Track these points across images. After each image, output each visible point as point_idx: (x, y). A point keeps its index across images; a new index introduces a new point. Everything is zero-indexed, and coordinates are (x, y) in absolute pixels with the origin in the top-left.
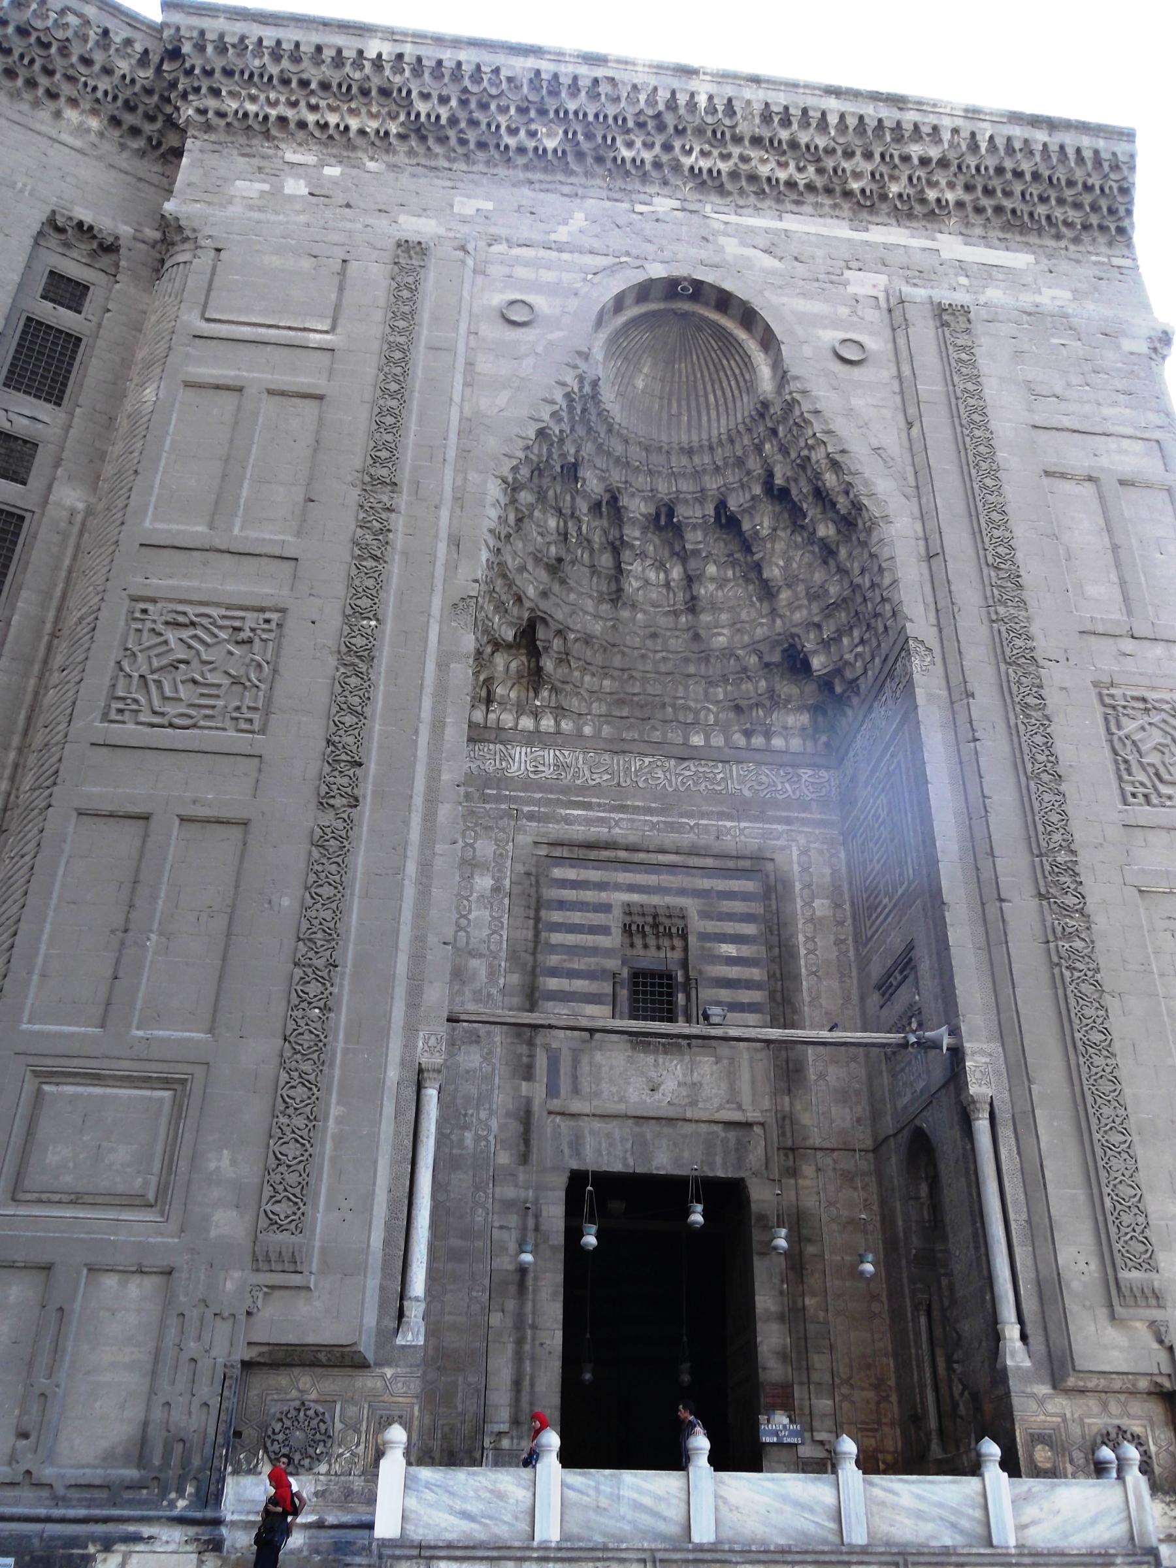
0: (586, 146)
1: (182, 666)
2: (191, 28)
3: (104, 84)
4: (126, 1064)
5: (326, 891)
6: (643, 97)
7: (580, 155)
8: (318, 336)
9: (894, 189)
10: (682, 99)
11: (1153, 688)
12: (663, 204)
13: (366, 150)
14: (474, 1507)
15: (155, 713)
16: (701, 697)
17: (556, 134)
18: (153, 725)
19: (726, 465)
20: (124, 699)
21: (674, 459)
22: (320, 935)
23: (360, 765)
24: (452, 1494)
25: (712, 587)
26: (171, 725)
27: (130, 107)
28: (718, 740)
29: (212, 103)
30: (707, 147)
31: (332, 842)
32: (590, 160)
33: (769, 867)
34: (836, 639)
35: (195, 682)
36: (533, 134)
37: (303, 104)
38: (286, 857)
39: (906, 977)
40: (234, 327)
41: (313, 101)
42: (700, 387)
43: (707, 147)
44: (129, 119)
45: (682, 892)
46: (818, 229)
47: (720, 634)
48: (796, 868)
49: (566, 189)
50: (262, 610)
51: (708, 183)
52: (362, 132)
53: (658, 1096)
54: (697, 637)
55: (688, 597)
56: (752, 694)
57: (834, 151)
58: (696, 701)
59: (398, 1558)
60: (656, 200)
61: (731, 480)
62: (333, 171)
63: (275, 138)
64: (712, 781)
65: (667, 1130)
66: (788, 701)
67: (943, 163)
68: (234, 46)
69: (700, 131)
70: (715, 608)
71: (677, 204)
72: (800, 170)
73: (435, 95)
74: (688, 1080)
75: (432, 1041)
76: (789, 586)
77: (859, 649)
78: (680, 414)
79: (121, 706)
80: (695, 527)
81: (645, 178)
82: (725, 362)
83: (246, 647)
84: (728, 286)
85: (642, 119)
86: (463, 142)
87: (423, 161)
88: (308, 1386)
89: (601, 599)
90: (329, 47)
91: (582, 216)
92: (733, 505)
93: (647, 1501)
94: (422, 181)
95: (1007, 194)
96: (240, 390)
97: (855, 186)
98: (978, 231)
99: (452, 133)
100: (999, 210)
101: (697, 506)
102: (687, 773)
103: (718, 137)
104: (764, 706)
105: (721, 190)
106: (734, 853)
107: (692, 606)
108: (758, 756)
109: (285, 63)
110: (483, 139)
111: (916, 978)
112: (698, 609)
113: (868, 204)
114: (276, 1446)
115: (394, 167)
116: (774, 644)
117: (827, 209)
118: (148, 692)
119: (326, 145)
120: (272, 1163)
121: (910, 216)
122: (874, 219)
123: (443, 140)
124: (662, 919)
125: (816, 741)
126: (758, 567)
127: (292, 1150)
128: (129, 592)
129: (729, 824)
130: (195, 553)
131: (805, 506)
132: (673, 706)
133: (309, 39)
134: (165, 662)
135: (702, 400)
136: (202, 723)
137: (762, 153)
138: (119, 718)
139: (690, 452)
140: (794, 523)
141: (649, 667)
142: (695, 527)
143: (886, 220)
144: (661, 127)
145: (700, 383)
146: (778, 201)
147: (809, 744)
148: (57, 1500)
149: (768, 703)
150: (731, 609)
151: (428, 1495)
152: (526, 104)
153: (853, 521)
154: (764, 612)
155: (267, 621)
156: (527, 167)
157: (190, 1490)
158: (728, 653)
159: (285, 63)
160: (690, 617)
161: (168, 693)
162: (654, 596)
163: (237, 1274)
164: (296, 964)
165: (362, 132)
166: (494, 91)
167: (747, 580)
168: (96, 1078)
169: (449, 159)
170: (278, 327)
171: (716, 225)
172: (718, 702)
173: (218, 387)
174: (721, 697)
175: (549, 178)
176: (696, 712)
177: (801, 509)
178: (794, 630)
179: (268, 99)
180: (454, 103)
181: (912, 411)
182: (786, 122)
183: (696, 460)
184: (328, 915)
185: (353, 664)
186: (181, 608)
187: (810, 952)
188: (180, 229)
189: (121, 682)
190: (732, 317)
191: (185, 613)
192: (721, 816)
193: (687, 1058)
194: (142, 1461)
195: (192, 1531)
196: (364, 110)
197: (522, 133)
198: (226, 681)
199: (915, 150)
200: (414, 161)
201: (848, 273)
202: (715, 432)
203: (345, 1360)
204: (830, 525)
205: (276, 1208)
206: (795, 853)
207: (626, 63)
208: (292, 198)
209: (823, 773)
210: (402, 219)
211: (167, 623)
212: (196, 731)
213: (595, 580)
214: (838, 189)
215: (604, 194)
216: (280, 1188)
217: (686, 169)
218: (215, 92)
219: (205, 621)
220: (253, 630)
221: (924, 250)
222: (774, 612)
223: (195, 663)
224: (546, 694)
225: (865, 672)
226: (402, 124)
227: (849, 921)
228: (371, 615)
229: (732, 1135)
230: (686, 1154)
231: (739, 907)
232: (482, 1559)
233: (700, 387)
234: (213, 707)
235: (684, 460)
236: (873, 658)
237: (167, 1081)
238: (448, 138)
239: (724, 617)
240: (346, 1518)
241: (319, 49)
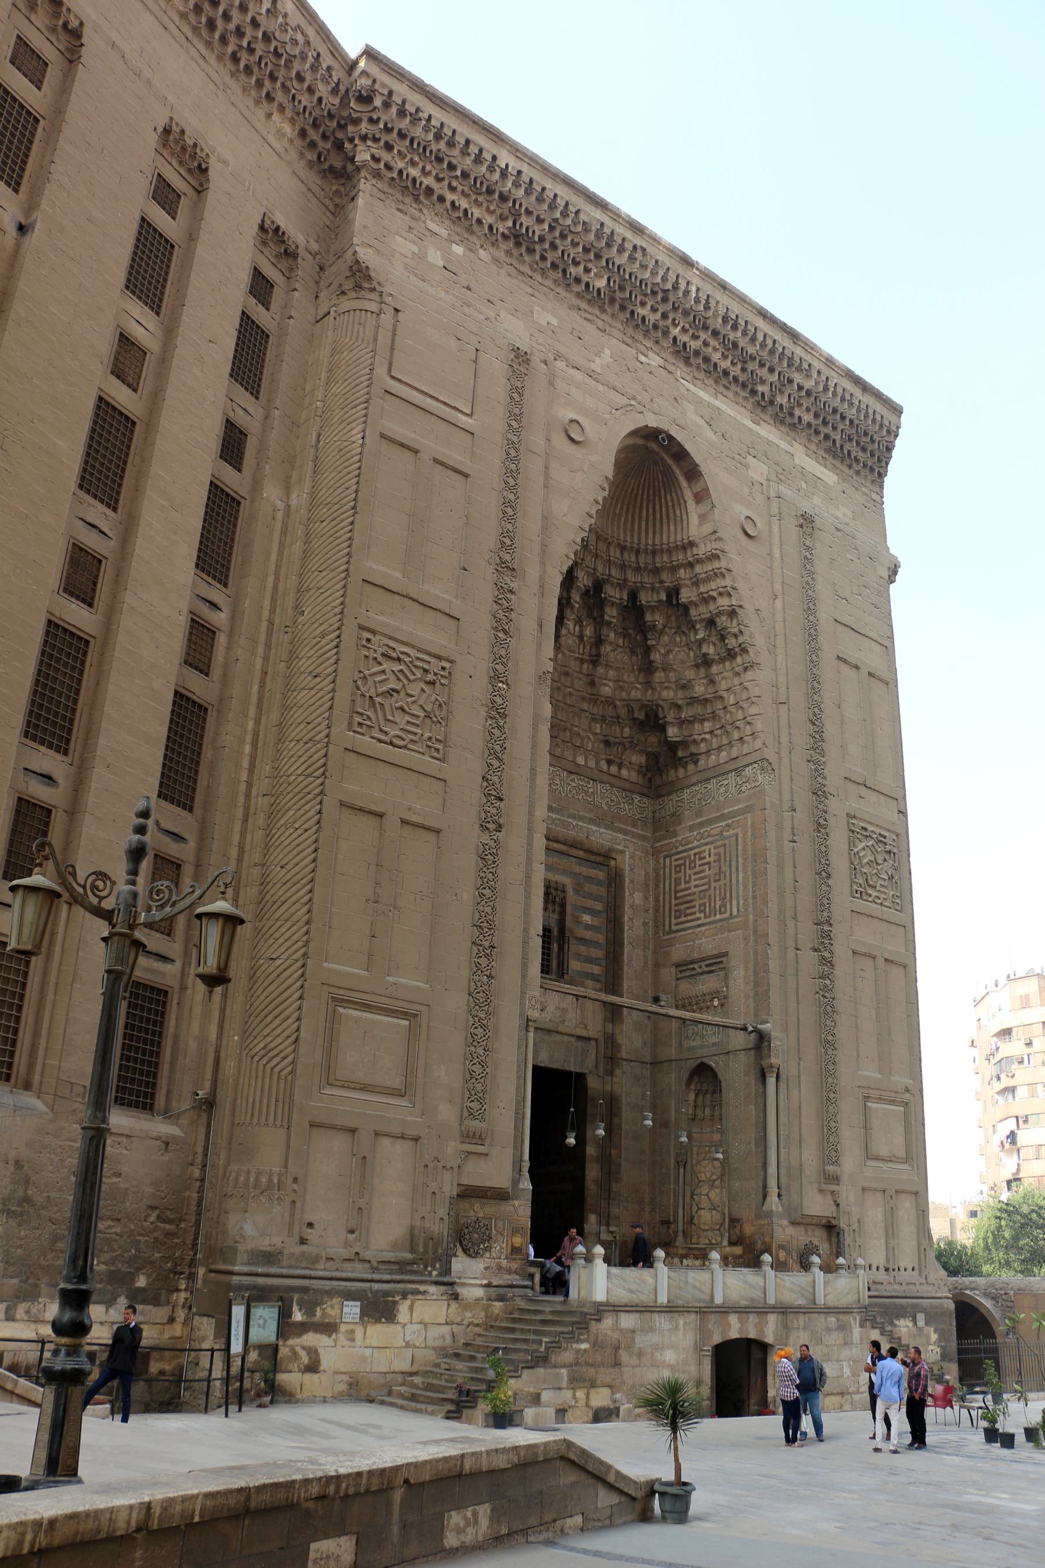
0: (618, 294)
1: (394, 694)
2: (384, 85)
3: (305, 100)
4: (384, 1000)
5: (487, 892)
6: (661, 273)
7: (612, 301)
8: (464, 418)
10: (683, 286)
11: (870, 823)
12: (654, 360)
13: (479, 237)
14: (633, 1287)
15: (381, 730)
16: (587, 728)
17: (602, 277)
18: (380, 741)
19: (646, 568)
20: (362, 714)
21: (612, 549)
22: (485, 924)
23: (501, 800)
24: (625, 1281)
25: (609, 648)
26: (391, 743)
27: (315, 125)
28: (592, 764)
29: (385, 156)
30: (687, 326)
31: (489, 857)
32: (617, 306)
33: (613, 863)
34: (691, 722)
35: (402, 709)
37: (446, 182)
38: (465, 865)
39: (712, 972)
40: (407, 389)
41: (454, 184)
42: (639, 500)
43: (687, 326)
44: (314, 135)
45: (564, 872)
46: (732, 410)
47: (607, 685)
48: (627, 868)
49: (600, 324)
50: (440, 658)
51: (682, 353)
52: (479, 221)
53: (544, 1015)
54: (592, 683)
55: (594, 652)
56: (619, 735)
57: (755, 358)
58: (584, 730)
59: (605, 1311)
60: (651, 354)
61: (646, 580)
62: (458, 249)
63: (421, 202)
64: (586, 792)
65: (547, 1037)
66: (637, 745)
67: (809, 393)
68: (411, 114)
69: (686, 313)
70: (608, 666)
71: (661, 362)
72: (732, 363)
73: (536, 213)
74: (562, 1006)
75: (533, 1002)
76: (664, 670)
77: (708, 736)
78: (620, 515)
79: (361, 721)
80: (613, 604)
81: (646, 334)
82: (662, 492)
83: (431, 687)
84: (689, 447)
85: (656, 289)
86: (543, 258)
87: (515, 263)
88: (479, 1210)
90: (476, 144)
91: (607, 351)
92: (644, 598)
93: (697, 1284)
94: (514, 281)
95: (834, 428)
96: (416, 452)
97: (760, 388)
98: (813, 447)
99: (538, 248)
100: (827, 437)
101: (617, 590)
102: (573, 784)
103: (698, 324)
105: (687, 361)
106: (596, 851)
107: (595, 660)
108: (613, 780)
109: (442, 145)
110: (557, 261)
111: (726, 975)
113: (764, 405)
114: (466, 1243)
115: (496, 260)
116: (643, 706)
117: (740, 400)
118: (376, 711)
119: (454, 222)
120: (468, 1077)
121: (782, 422)
122: (762, 416)
123: (531, 251)
124: (553, 891)
125: (644, 775)
126: (648, 650)
127: (477, 1068)
128: (358, 621)
129: (594, 828)
130: (397, 597)
131: (698, 626)
132: (571, 730)
133: (465, 132)
134: (384, 689)
135: (637, 510)
136: (410, 746)
137: (716, 343)
138: (359, 730)
139: (623, 548)
140: (679, 627)
141: (560, 698)
142: (613, 604)
143: (767, 418)
144: (665, 300)
145: (639, 497)
146: (716, 382)
147: (640, 777)
148: (375, 1270)
149: (628, 745)
150: (617, 669)
151: (616, 1281)
152: (588, 246)
154: (641, 680)
155: (443, 668)
156: (578, 295)
157: (438, 1266)
158: (610, 702)
159: (442, 145)
160: (591, 667)
161: (390, 718)
162: (570, 642)
163: (453, 1143)
164: (473, 943)
165: (479, 221)
166: (572, 229)
167: (633, 652)
168: (367, 1007)
169: (531, 267)
170: (437, 400)
171: (683, 390)
173: (402, 445)
174: (598, 731)
175: (590, 310)
176: (582, 739)
177: (694, 627)
178: (661, 702)
179: (424, 168)
180: (546, 227)
182: (735, 327)
183: (626, 555)
184: (488, 910)
185: (495, 718)
186: (392, 644)
187: (630, 928)
189: (359, 700)
190: (680, 467)
191: (394, 649)
192: (591, 821)
194: (412, 1250)
195: (443, 1288)
196: (485, 205)
197: (581, 267)
198: (422, 714)
199: (798, 378)
200: (509, 261)
201: (750, 458)
202: (643, 541)
203: (501, 1196)
204: (712, 647)
205: (472, 1105)
206: (627, 857)
207: (655, 240)
208: (432, 266)
209: (645, 800)
210: (503, 314)
211: (383, 654)
212: (407, 752)
214: (750, 387)
215: (621, 336)
216: (473, 1092)
217: (671, 336)
218: (389, 147)
219: (407, 659)
220: (435, 674)
221: (787, 452)
222: (648, 684)
223: (402, 693)
225: (708, 752)
226: (508, 228)
227: (651, 911)
228: (504, 679)
229: (580, 1044)
230: (556, 1054)
231: (593, 889)
232: (637, 1311)
233: (639, 500)
234: (416, 734)
235: (618, 554)
236: (719, 748)
237: (406, 1014)
238: (534, 250)
239: (611, 673)
240: (501, 1282)
241: (468, 142)
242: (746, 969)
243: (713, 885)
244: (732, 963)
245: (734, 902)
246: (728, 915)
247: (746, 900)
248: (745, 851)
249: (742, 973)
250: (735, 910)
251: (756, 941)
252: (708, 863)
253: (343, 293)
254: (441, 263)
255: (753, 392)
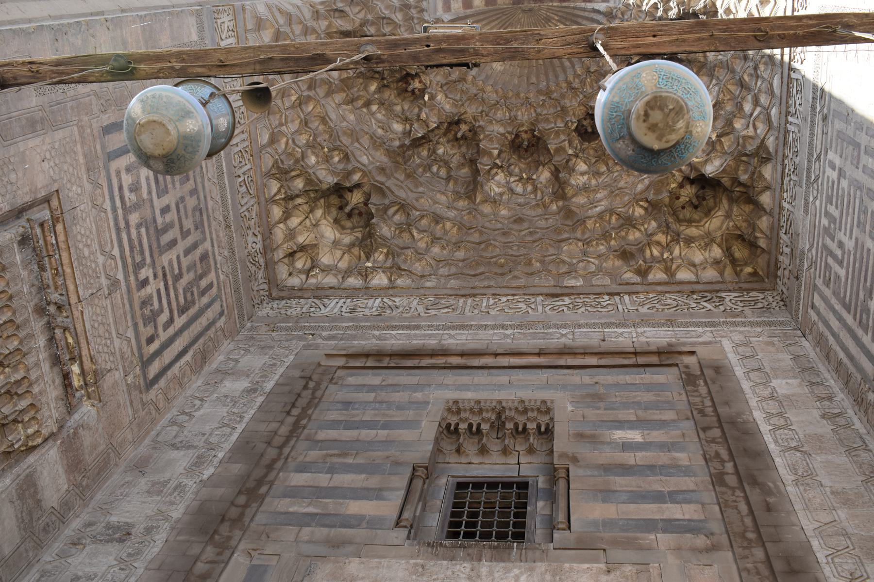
89: (458, 196)
104: (658, 243)
112: (569, 195)
172: (599, 256)
193: (541, 567)
213: (451, 185)
224: (381, 257)
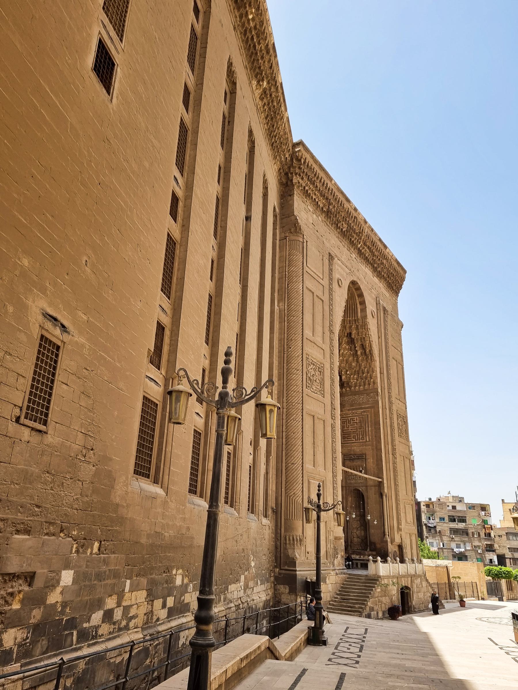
9: (379, 269)
36: (342, 224)
51: (360, 253)
97: (375, 266)
153: (368, 355)
181: (380, 334)
188: (300, 229)
218: (302, 179)
242: (373, 459)
243: (358, 430)
244: (367, 457)
245: (367, 437)
246: (365, 441)
247: (372, 437)
248: (371, 421)
249: (372, 461)
250: (368, 440)
251: (377, 451)
252: (356, 423)
253: (291, 232)
254: (312, 222)
255: (374, 266)
